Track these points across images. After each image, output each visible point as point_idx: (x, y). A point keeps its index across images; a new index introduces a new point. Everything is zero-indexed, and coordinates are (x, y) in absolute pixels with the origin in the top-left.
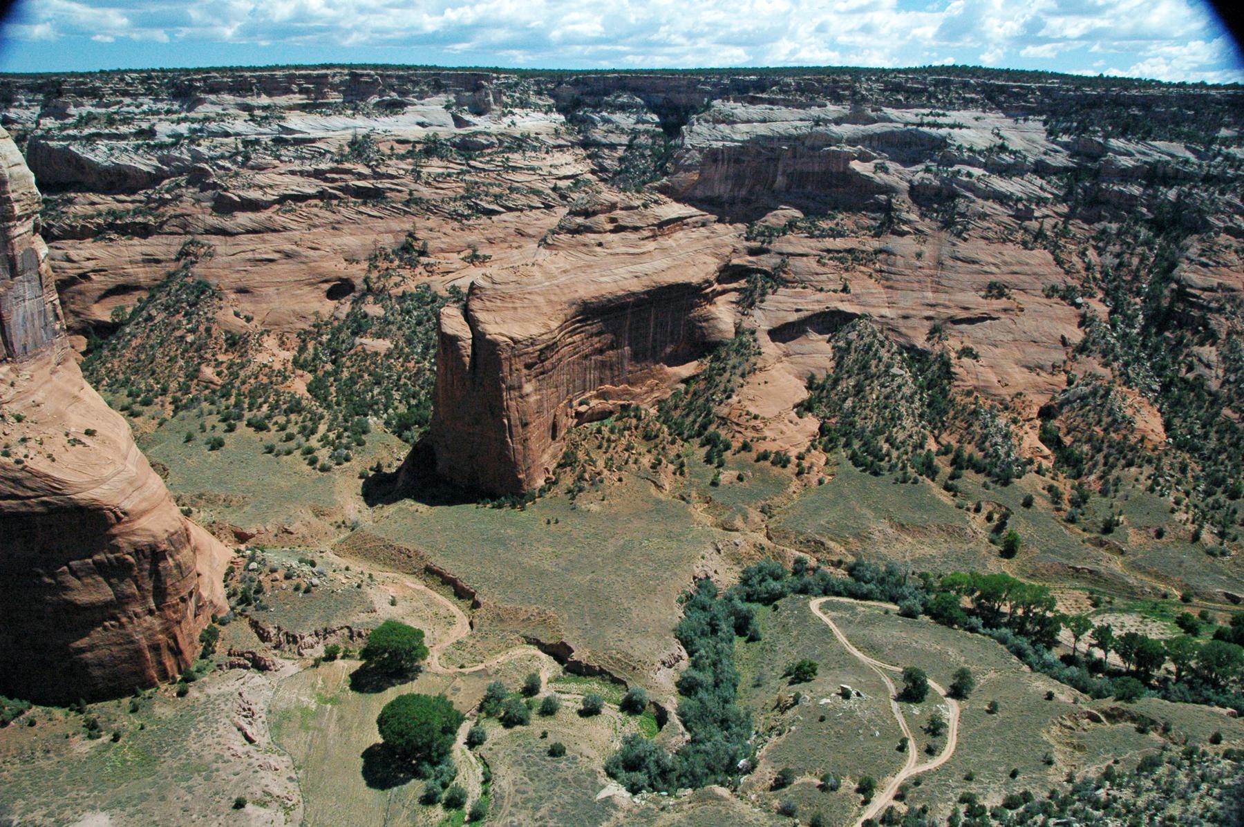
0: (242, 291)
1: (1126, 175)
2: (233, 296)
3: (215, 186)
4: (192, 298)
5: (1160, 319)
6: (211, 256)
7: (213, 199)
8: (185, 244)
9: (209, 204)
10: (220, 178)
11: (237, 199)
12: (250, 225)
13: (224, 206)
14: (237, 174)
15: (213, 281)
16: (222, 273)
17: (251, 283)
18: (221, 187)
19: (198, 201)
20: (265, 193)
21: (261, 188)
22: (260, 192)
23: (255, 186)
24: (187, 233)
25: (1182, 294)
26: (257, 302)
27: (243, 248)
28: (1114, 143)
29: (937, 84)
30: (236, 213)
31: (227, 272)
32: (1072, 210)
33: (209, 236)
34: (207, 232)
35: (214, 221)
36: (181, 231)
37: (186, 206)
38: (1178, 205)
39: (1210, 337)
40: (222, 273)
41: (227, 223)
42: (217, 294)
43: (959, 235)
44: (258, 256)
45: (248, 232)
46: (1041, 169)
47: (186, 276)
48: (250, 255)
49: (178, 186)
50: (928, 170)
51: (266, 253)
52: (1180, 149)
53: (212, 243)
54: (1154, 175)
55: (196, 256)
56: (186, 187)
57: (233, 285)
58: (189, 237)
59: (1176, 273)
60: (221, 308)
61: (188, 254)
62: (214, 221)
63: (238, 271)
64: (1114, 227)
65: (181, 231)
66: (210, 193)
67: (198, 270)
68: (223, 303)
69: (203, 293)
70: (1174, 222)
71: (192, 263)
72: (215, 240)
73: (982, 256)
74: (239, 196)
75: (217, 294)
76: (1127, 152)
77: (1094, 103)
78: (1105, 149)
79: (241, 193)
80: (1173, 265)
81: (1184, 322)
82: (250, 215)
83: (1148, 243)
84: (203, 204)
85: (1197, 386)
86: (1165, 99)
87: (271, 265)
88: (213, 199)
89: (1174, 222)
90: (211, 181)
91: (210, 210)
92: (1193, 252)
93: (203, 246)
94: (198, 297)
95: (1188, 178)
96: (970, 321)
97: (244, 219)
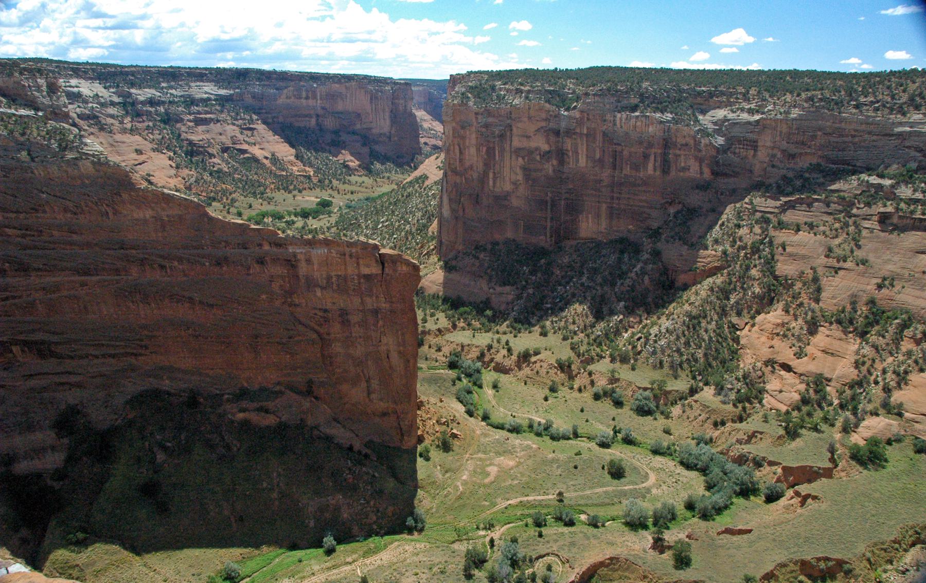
1: (142, 103)
5: (191, 153)
25: (191, 143)
28: (133, 91)
29: (57, 67)
32: (132, 119)
38: (167, 113)
39: (211, 156)
43: (110, 132)
46: (113, 104)
50: (79, 107)
52: (153, 91)
54: (151, 102)
59: (182, 137)
64: (151, 124)
70: (168, 120)
73: (125, 140)
76: (142, 94)
77: (114, 74)
78: (130, 94)
80: (180, 135)
81: (199, 153)
83: (165, 128)
85: (219, 171)
86: (138, 72)
89: (168, 120)
92: (183, 129)
95: (163, 103)
96: (140, 164)
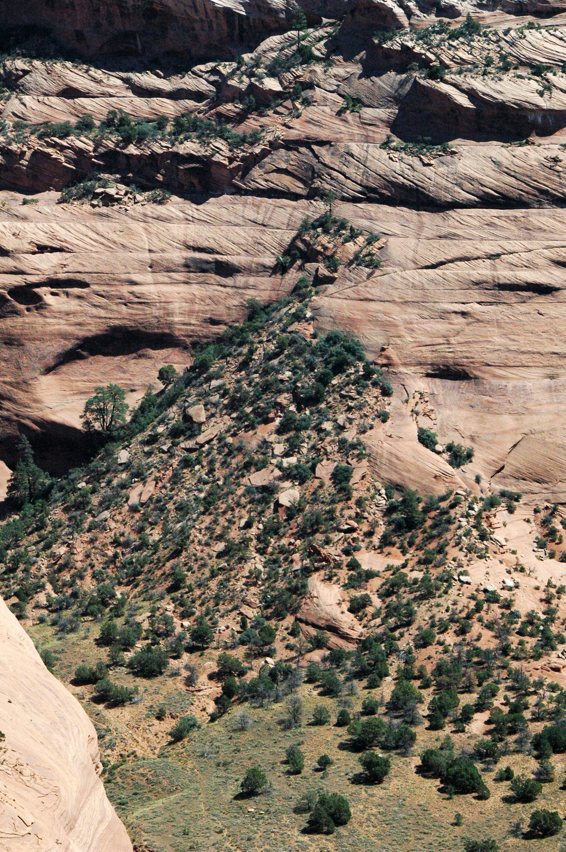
0: (449, 372)
2: (421, 384)
3: (405, 60)
4: (307, 382)
6: (374, 265)
7: (397, 100)
8: (306, 227)
9: (383, 113)
10: (423, 36)
11: (463, 100)
12: (493, 180)
13: (426, 121)
14: (472, 28)
15: (371, 337)
16: (398, 315)
17: (478, 352)
18: (425, 63)
19: (355, 103)
20: (548, 87)
21: (538, 70)
22: (535, 85)
23: (522, 63)
24: (314, 194)
26: (488, 409)
27: (467, 248)
30: (456, 144)
31: (412, 313)
33: (372, 208)
34: (371, 195)
35: (400, 165)
36: (298, 187)
37: (320, 117)
40: (398, 315)
41: (432, 173)
42: (377, 377)
44: (505, 274)
45: (487, 201)
47: (298, 317)
48: (483, 271)
49: (305, 56)
51: (530, 266)
53: (378, 227)
55: (332, 262)
56: (327, 61)
57: (427, 354)
58: (319, 207)
60: (384, 417)
61: (310, 255)
62: (400, 165)
63: (444, 315)
65: (298, 187)
66: (389, 80)
67: (334, 303)
68: (392, 404)
69: (339, 368)
71: (320, 281)
72: (388, 219)
74: (472, 94)
75: (377, 377)
79: (478, 84)
82: (495, 149)
84: (368, 113)
87: (541, 303)
88: (397, 100)
90: (394, 44)
91: (383, 132)
93: (353, 235)
94: (323, 380)
97: (476, 160)
